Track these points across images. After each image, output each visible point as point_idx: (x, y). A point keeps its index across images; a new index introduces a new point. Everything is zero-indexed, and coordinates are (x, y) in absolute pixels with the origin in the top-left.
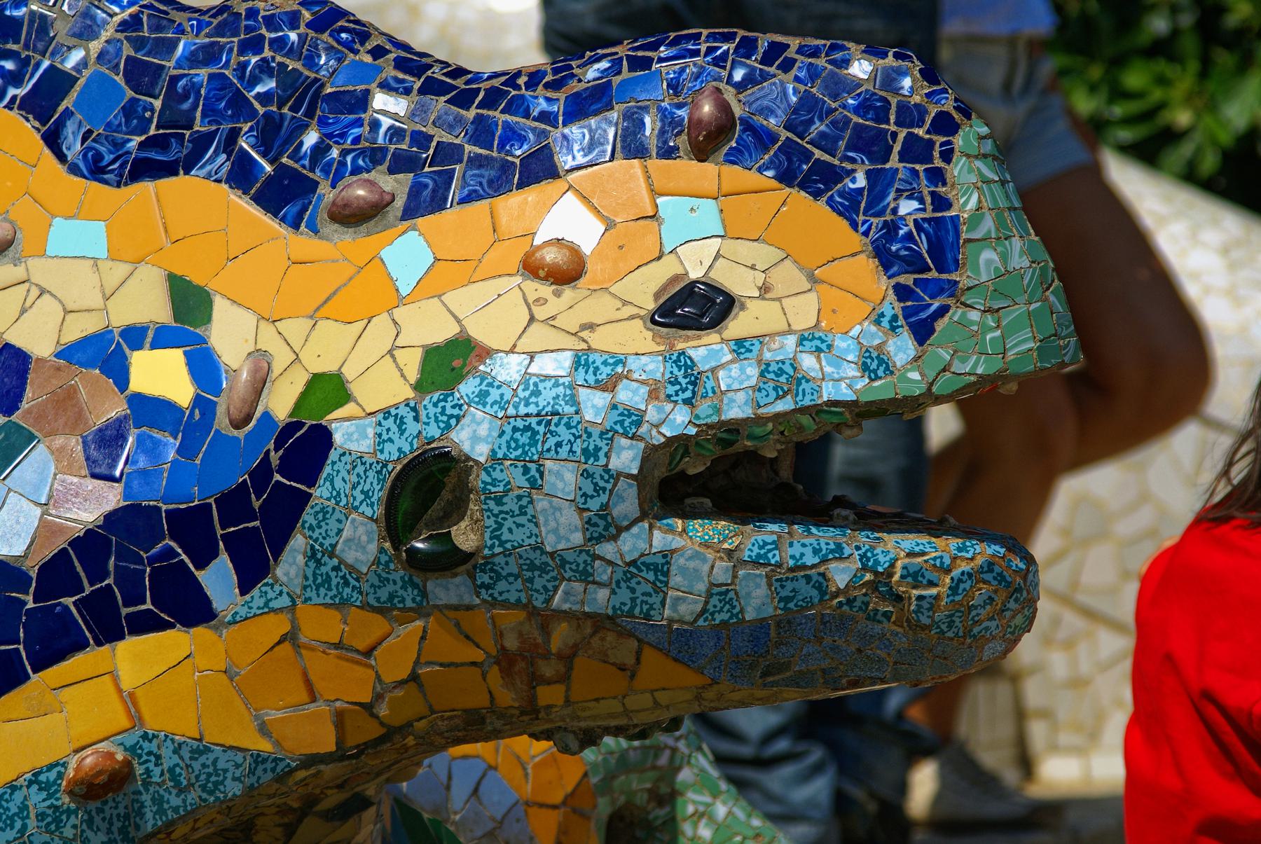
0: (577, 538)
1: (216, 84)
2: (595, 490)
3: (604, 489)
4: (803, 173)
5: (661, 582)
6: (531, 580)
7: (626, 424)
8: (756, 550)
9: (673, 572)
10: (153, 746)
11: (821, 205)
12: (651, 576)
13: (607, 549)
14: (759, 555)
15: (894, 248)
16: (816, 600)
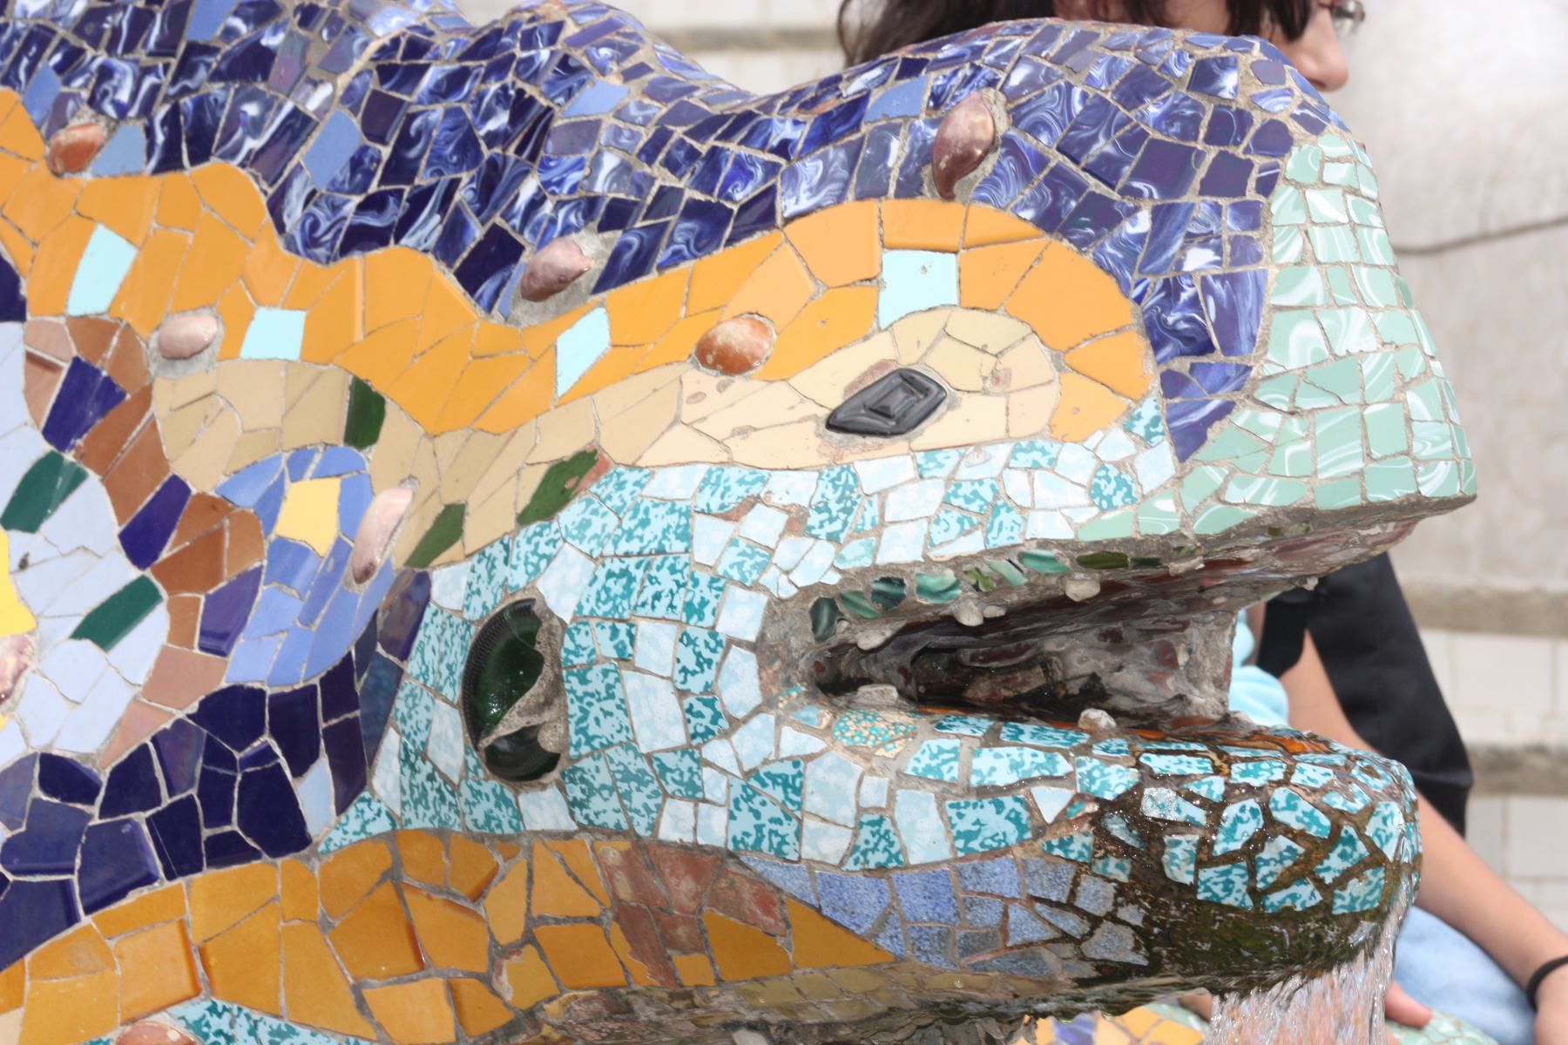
0: (678, 736)
1: (450, 122)
2: (699, 664)
3: (709, 662)
4: (1070, 214)
5: (793, 803)
6: (627, 795)
7: (746, 567)
8: (925, 760)
9: (809, 788)
10: (223, 1023)
12: (778, 793)
13: (716, 751)
14: (929, 769)
15: (1171, 320)
16: (1012, 838)
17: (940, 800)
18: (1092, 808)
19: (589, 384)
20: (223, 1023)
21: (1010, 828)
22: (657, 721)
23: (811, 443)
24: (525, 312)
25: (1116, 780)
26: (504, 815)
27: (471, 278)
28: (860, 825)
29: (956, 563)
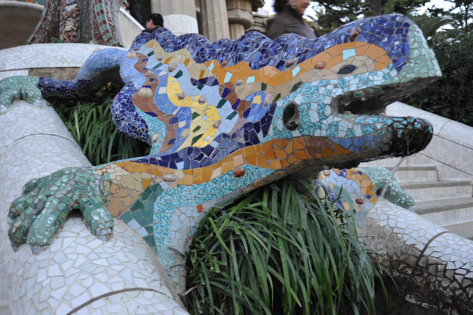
0: (318, 120)
6: (309, 130)
8: (358, 121)
9: (339, 126)
10: (248, 167)
11: (377, 47)
12: (334, 127)
13: (324, 121)
17: (361, 126)
18: (386, 126)
19: (298, 75)
20: (248, 167)
21: (373, 131)
22: (314, 117)
24: (287, 70)
26: (289, 135)
28: (348, 131)
29: (362, 90)
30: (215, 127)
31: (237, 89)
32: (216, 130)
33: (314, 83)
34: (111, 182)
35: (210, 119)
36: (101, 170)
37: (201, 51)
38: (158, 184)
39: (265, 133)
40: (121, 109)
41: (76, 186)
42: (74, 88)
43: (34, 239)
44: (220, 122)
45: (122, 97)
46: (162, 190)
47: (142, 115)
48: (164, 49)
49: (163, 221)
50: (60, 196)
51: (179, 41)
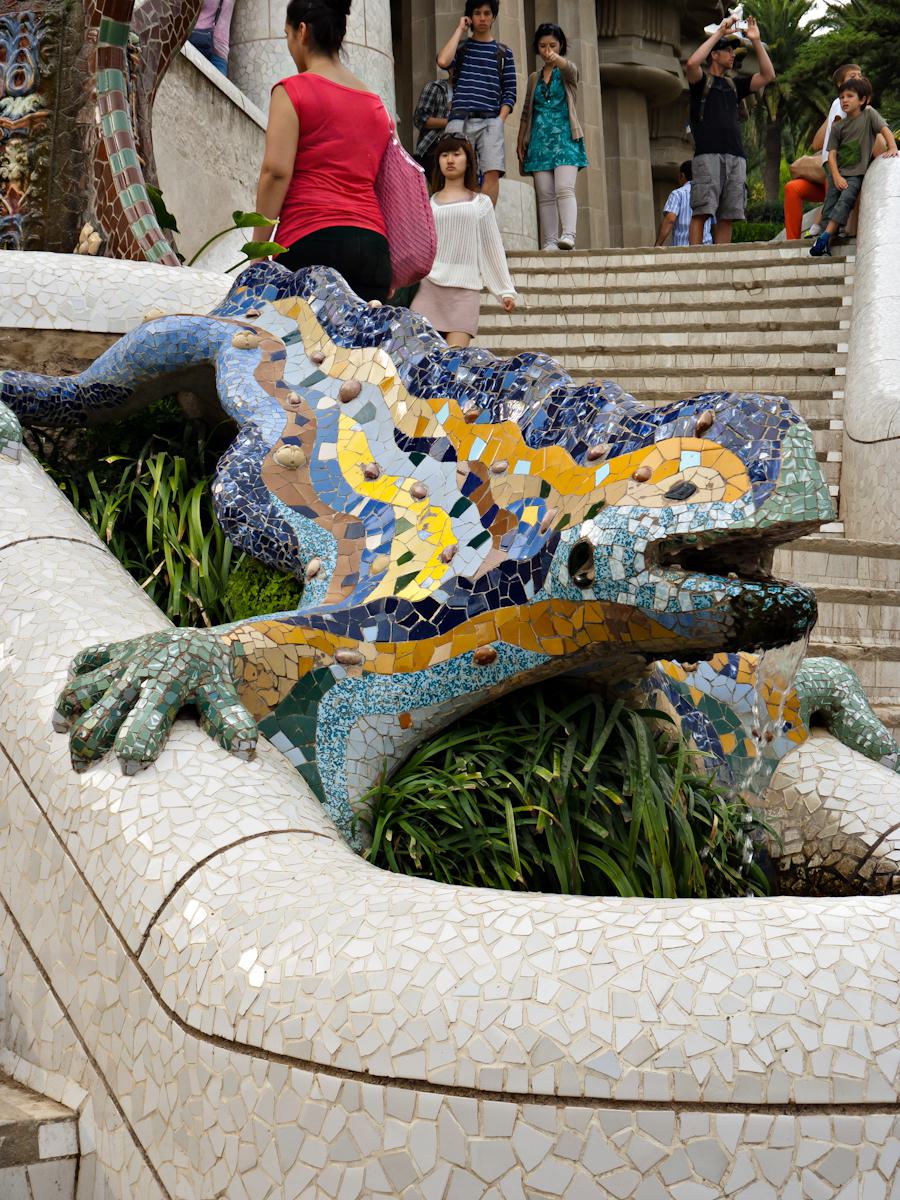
0: (623, 576)
11: (734, 456)
13: (633, 580)
22: (618, 572)
23: (659, 501)
25: (737, 591)
26: (578, 595)
27: (574, 454)
29: (697, 533)
30: (446, 560)
31: (495, 482)
32: (446, 566)
33: (624, 511)
34: (245, 659)
35: (434, 539)
36: (228, 635)
37: (420, 365)
38: (327, 668)
39: (538, 586)
40: (239, 497)
41: (192, 663)
42: (78, 398)
43: (131, 749)
44: (454, 551)
45: (239, 466)
46: (333, 681)
47: (285, 513)
48: (330, 335)
49: (334, 739)
50: (169, 679)
51: (368, 322)
